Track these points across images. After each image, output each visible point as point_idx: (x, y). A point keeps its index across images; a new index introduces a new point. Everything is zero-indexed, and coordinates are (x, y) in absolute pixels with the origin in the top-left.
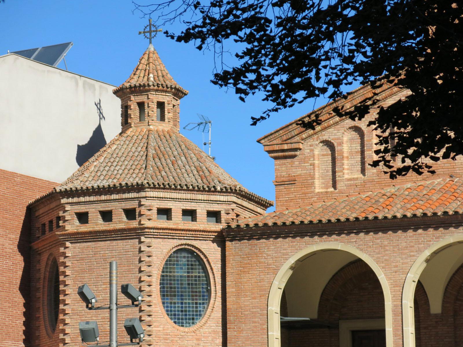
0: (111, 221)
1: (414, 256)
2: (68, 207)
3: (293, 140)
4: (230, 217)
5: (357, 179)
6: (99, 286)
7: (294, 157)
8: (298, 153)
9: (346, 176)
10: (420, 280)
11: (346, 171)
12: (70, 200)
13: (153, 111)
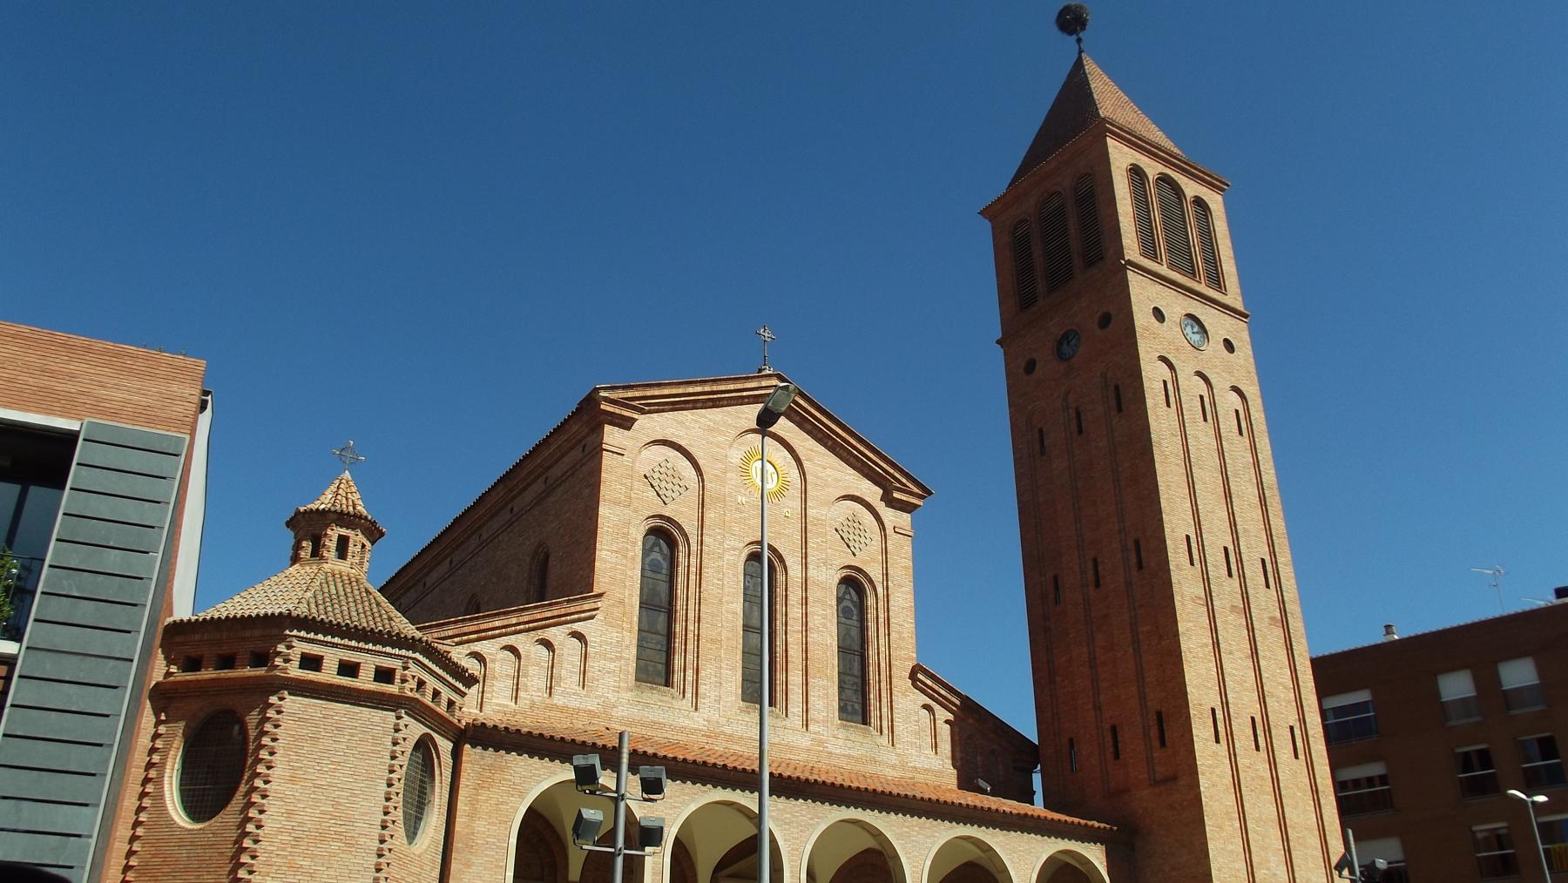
0: (357, 678)
1: (679, 808)
2: (295, 643)
3: (445, 642)
5: (507, 706)
6: (324, 765)
10: (679, 836)
12: (303, 634)
13: (330, 551)
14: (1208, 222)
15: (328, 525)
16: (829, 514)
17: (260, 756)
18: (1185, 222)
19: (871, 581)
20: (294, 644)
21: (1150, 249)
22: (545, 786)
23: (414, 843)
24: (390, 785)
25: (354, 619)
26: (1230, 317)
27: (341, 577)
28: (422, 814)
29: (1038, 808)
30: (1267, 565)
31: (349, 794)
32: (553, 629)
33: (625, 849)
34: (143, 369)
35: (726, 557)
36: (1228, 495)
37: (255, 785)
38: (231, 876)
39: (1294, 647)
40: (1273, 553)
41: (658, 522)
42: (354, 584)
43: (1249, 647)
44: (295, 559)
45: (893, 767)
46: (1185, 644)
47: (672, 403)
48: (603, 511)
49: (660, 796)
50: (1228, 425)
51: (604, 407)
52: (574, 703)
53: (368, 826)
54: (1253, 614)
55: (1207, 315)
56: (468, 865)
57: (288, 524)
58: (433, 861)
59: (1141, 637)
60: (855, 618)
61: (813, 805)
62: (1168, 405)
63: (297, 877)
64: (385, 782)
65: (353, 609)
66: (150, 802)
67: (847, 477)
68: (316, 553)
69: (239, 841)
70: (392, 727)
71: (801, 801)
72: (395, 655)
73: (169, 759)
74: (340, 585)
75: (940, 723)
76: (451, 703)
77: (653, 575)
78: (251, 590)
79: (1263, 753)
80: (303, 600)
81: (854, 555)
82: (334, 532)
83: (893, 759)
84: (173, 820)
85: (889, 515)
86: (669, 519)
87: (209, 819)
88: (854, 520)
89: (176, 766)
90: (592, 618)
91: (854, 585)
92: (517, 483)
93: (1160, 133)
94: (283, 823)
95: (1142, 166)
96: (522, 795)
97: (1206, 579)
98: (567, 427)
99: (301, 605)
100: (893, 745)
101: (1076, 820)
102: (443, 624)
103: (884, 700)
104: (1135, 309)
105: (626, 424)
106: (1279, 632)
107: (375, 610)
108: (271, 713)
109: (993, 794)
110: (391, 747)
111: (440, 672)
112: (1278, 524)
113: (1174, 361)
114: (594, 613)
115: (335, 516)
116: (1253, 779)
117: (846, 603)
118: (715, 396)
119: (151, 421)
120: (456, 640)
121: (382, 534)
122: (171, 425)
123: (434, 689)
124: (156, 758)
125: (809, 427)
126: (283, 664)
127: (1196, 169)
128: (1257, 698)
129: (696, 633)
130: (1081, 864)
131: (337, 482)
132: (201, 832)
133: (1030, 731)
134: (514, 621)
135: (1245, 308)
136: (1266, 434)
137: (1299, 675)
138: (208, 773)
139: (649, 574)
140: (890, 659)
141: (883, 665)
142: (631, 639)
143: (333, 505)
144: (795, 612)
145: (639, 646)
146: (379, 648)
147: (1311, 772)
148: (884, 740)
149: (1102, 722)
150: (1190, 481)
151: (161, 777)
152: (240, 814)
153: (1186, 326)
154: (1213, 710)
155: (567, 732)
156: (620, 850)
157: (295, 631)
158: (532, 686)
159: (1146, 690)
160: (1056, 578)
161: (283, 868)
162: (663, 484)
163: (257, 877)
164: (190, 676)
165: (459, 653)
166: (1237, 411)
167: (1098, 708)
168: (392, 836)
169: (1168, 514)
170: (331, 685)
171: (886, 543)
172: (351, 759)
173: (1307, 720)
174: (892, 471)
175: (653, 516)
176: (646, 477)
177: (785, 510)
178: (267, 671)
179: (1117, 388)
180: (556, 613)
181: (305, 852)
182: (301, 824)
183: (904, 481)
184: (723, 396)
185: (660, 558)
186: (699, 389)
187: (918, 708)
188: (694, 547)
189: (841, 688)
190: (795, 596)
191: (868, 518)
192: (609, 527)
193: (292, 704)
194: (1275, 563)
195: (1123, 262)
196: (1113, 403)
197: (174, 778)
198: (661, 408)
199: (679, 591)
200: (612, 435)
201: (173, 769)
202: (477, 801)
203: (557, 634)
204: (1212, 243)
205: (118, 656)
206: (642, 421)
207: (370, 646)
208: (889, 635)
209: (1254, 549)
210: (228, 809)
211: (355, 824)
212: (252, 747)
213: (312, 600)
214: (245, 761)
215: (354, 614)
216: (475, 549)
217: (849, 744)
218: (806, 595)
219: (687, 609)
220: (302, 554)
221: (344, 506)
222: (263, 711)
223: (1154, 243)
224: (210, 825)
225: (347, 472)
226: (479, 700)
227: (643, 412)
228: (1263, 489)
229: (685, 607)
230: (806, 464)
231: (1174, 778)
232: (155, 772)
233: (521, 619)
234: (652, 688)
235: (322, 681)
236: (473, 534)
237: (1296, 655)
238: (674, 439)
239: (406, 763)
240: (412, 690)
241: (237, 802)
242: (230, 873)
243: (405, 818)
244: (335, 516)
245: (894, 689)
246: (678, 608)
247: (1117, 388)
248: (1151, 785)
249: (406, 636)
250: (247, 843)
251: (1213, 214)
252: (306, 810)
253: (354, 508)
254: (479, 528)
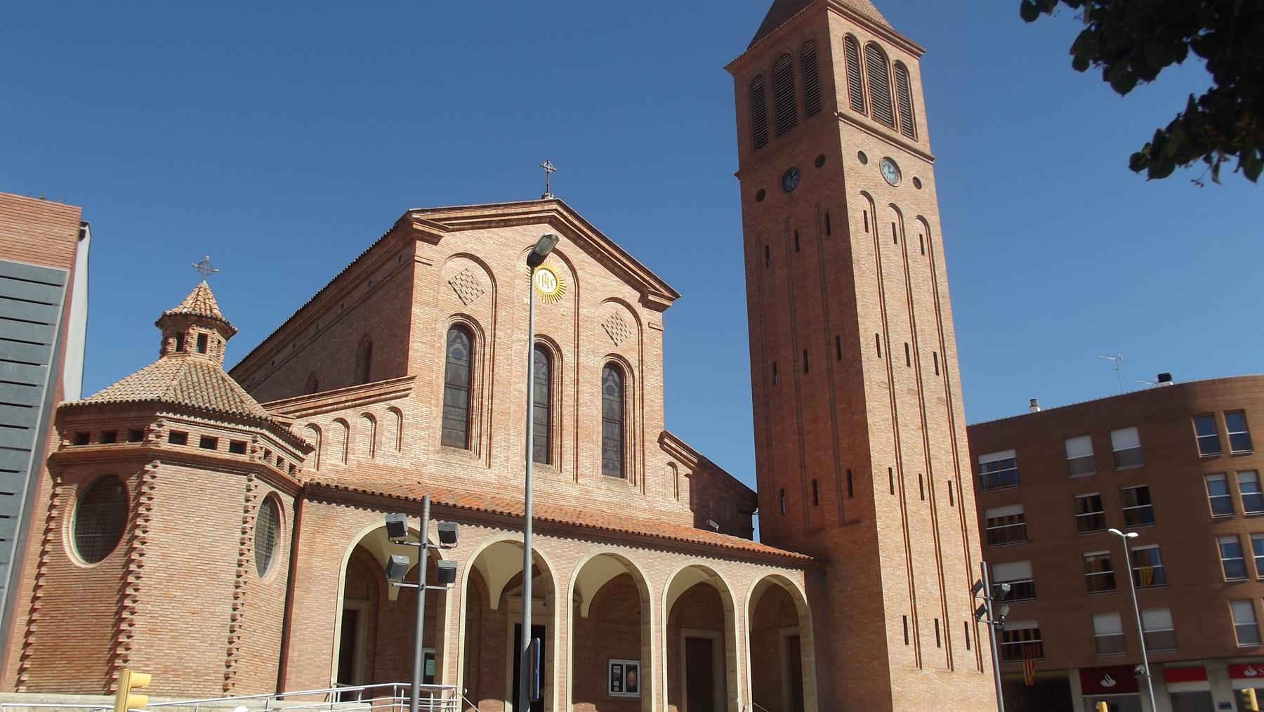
2: (165, 422)
3: (288, 416)
12: (171, 415)
14: (906, 82)
15: (190, 326)
16: (596, 312)
17: (139, 512)
18: (887, 81)
19: (629, 366)
20: (164, 423)
21: (858, 105)
22: (368, 530)
23: (265, 575)
24: (244, 533)
25: (212, 402)
26: (919, 160)
27: (201, 367)
28: (270, 553)
29: (755, 543)
30: (938, 357)
31: (211, 540)
32: (375, 406)
33: (427, 585)
34: (29, 214)
35: (514, 347)
36: (910, 302)
37: (136, 534)
38: (119, 605)
39: (955, 421)
40: (943, 348)
41: (460, 319)
42: (212, 373)
43: (920, 421)
44: (164, 353)
45: (644, 511)
46: (871, 419)
47: (472, 223)
48: (416, 310)
49: (455, 545)
50: (913, 246)
51: (416, 226)
52: (392, 463)
53: (227, 564)
54: (925, 396)
55: (902, 158)
56: (308, 592)
57: (157, 324)
58: (280, 590)
59: (838, 412)
60: (616, 394)
61: (579, 542)
62: (867, 230)
63: (171, 604)
64: (240, 530)
65: (212, 394)
66: (51, 547)
67: (612, 283)
68: (180, 348)
69: (124, 577)
70: (245, 487)
71: (569, 539)
72: (246, 431)
73: (65, 514)
74: (200, 374)
75: (681, 476)
76: (292, 467)
77: (455, 361)
78: (128, 379)
79: (927, 502)
80: (171, 388)
81: (617, 345)
82: (195, 332)
83: (644, 505)
84: (70, 561)
85: (645, 314)
86: (469, 317)
87: (100, 560)
88: (617, 317)
89: (72, 519)
90: (406, 396)
91: (616, 369)
92: (347, 284)
93: (872, 7)
94: (160, 563)
95: (855, 34)
96: (350, 538)
97: (890, 368)
98: (386, 241)
99: (168, 392)
100: (644, 494)
101: (782, 552)
102: (286, 402)
103: (638, 459)
104: (844, 152)
105: (434, 240)
106: (944, 409)
107: (230, 395)
108: (147, 478)
109: (720, 531)
110: (244, 503)
111: (283, 443)
112: (948, 325)
113: (873, 195)
114: (408, 392)
115: (195, 318)
116: (917, 521)
117: (610, 383)
118: (506, 218)
119: (37, 257)
120: (297, 414)
121: (234, 332)
122: (55, 260)
123: (279, 457)
124: (55, 513)
125: (582, 243)
126: (155, 439)
127: (899, 38)
128: (924, 460)
129: (490, 407)
130: (786, 585)
131: (197, 290)
132: (94, 570)
133: (751, 483)
134: (344, 399)
135: (932, 153)
136: (943, 254)
137: (958, 442)
138: (97, 524)
139: (452, 360)
140: (643, 427)
141: (637, 432)
142: (437, 412)
143: (194, 309)
144: (569, 390)
145: (445, 418)
146: (233, 425)
147: (962, 516)
148: (637, 490)
149: (806, 477)
150: (881, 292)
151: (59, 527)
152: (124, 557)
153: (884, 166)
154: (890, 469)
155: (386, 487)
156: (423, 586)
157: (165, 413)
158: (359, 450)
159: (840, 453)
160: (775, 364)
161: (160, 598)
162: (464, 289)
163: (140, 605)
164: (80, 448)
165: (299, 425)
166: (921, 236)
167: (803, 466)
168: (246, 572)
169: (863, 317)
170: (195, 456)
171: (642, 336)
172: (213, 513)
173: (962, 477)
174: (648, 279)
175: (456, 315)
176: (450, 283)
177: (562, 310)
178: (143, 445)
179: (827, 216)
180: (377, 392)
181: (178, 585)
182: (174, 563)
183: (657, 286)
184: (513, 217)
185: (461, 348)
186: (493, 212)
187: (664, 465)
188: (488, 339)
189: (604, 450)
190: (569, 377)
191: (628, 315)
192: (420, 323)
193: (163, 470)
194: (944, 356)
195: (836, 115)
196: (824, 227)
197: (70, 529)
198: (462, 228)
199: (476, 374)
200: (422, 249)
201: (69, 522)
202: (315, 543)
203: (378, 409)
204: (908, 99)
205: (18, 447)
206: (447, 238)
207: (226, 424)
208: (643, 408)
209: (929, 344)
210: (114, 553)
211: (217, 563)
212: (132, 505)
213: (178, 388)
214: (127, 515)
215: (212, 398)
216: (314, 337)
217: (610, 493)
218: (578, 377)
219: (482, 389)
220: (169, 349)
221: (203, 310)
222: (141, 476)
223: (862, 99)
224: (100, 566)
225: (205, 282)
226: (316, 462)
227: (447, 230)
228: (938, 297)
229: (481, 387)
230: (579, 273)
231: (858, 521)
232: (54, 524)
233: (349, 398)
234: (454, 451)
235: (188, 452)
236: (312, 323)
237: (956, 427)
238: (473, 253)
239: (257, 515)
240: (260, 458)
241: (122, 547)
242: (118, 602)
243: (257, 557)
244: (195, 318)
245: (646, 453)
246: (476, 387)
247: (827, 216)
248: (840, 526)
249: (254, 416)
250: (131, 579)
251: (911, 75)
252: (178, 553)
253: (211, 312)
254: (318, 319)
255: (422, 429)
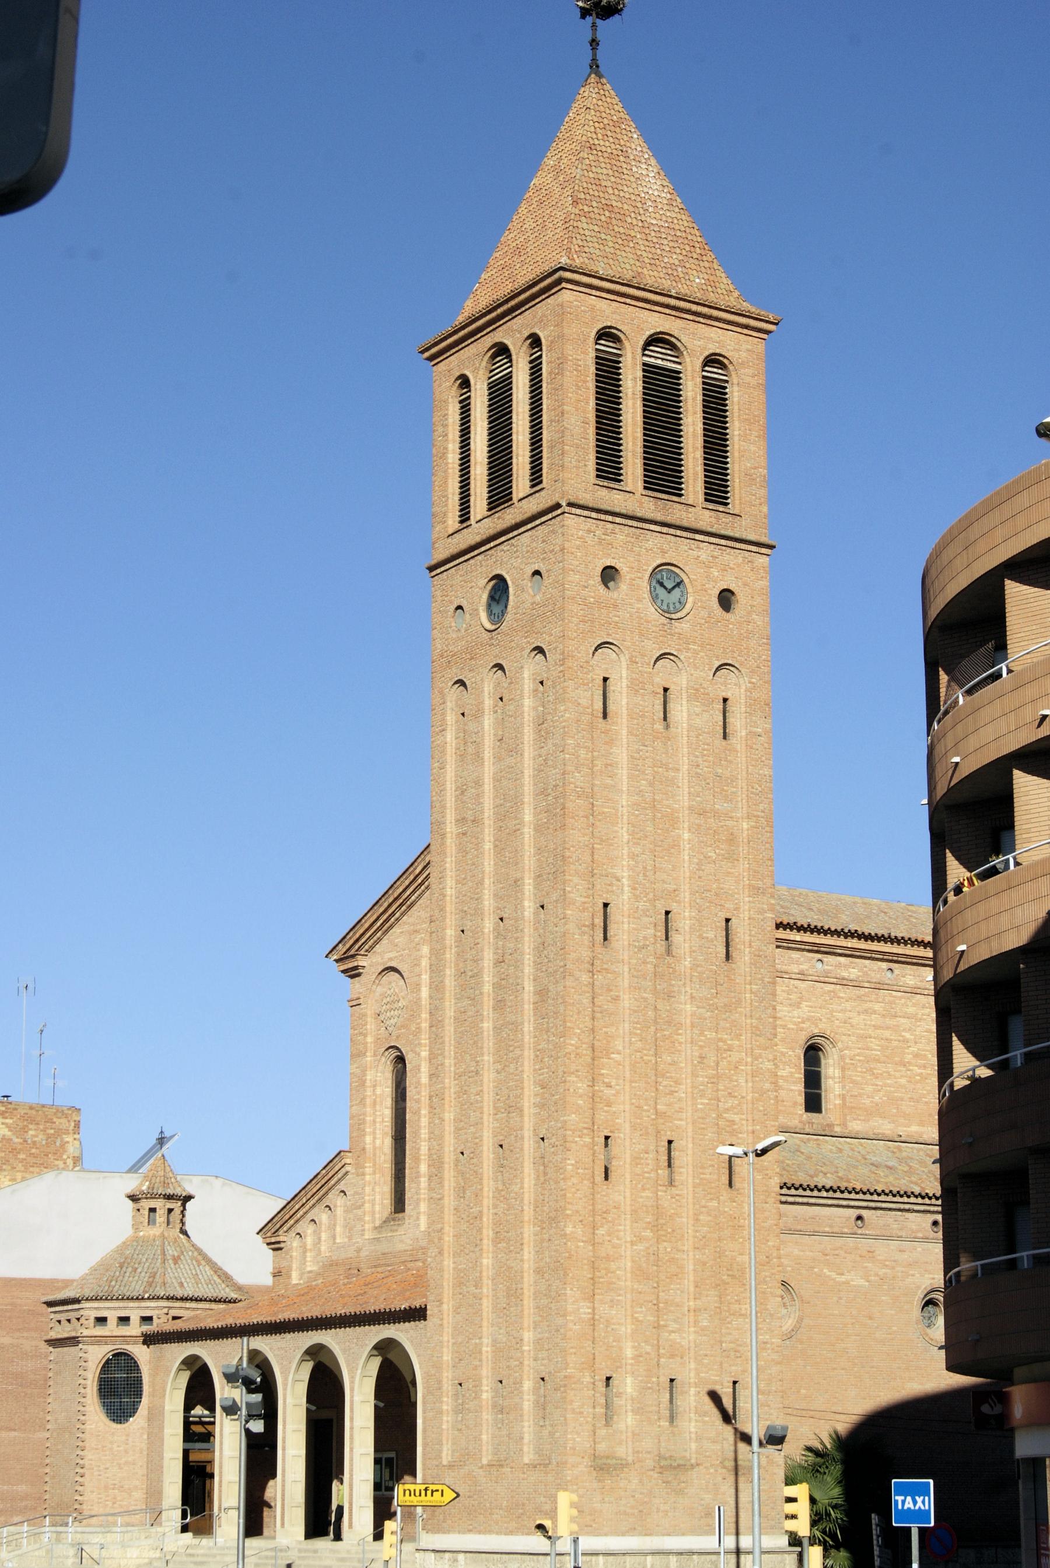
4: (161, 1321)
7: (280, 1249)
8: (282, 1245)
9: (309, 1269)
11: (308, 1264)
32: (330, 1195)
255: (359, 1207)
